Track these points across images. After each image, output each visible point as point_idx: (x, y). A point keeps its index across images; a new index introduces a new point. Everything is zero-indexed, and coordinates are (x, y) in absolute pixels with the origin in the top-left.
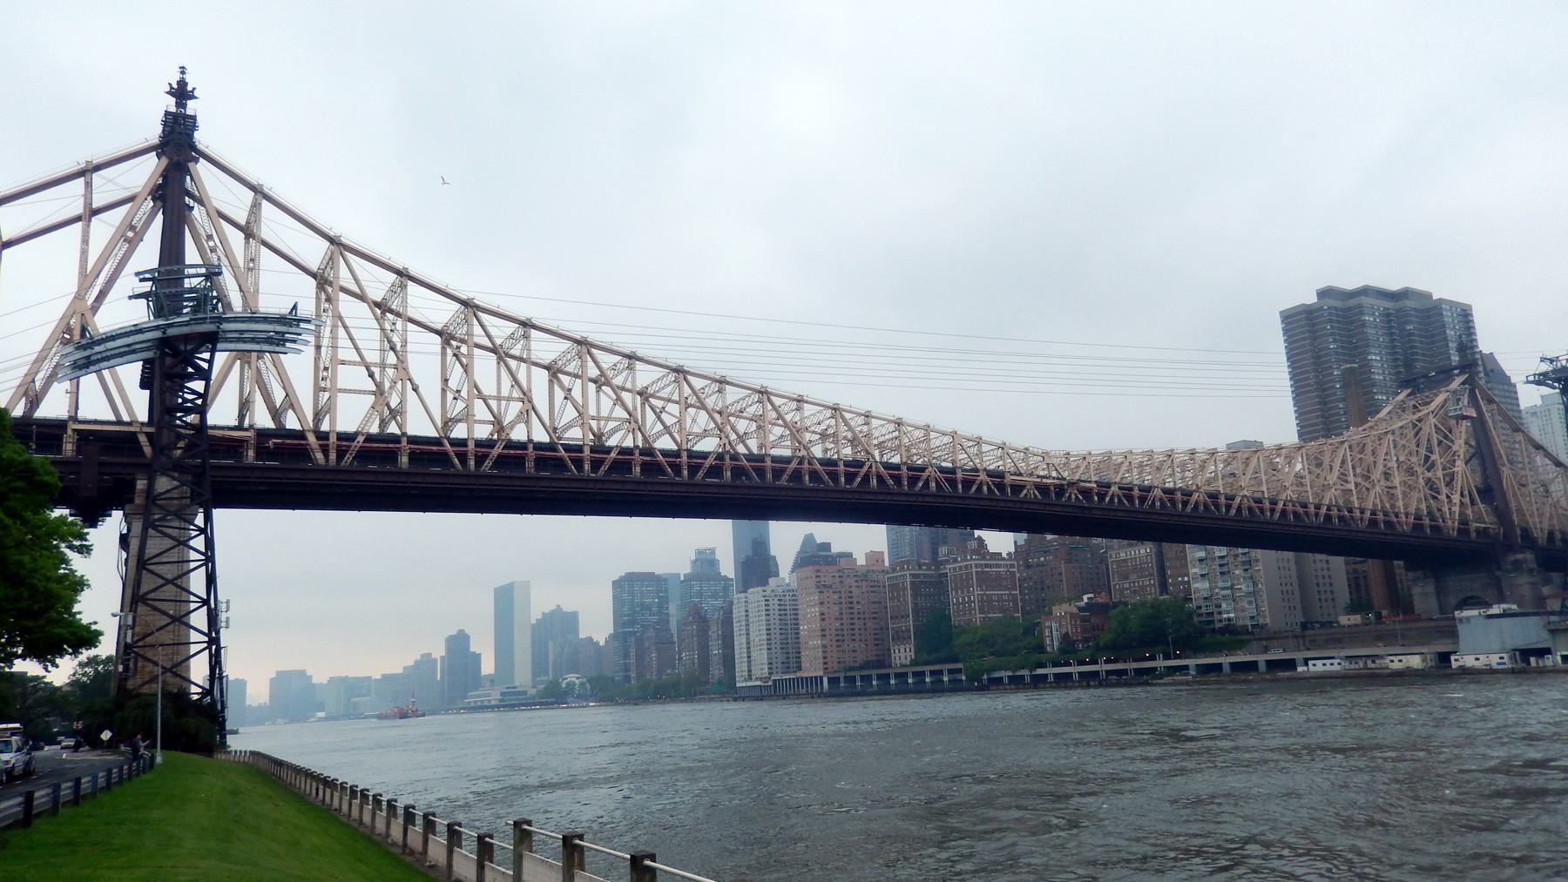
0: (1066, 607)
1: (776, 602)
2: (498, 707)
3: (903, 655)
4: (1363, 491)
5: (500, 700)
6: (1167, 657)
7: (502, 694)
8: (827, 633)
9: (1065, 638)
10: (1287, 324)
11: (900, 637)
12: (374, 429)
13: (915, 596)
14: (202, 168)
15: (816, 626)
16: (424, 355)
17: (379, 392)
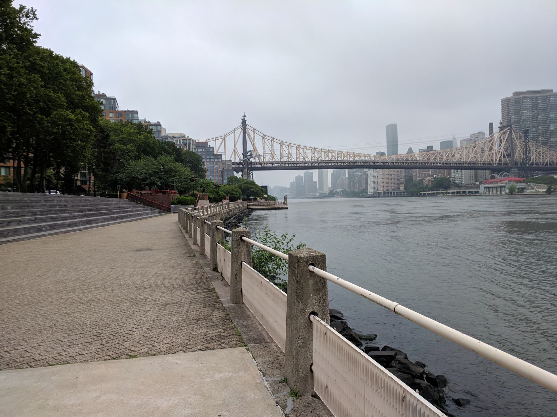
0: (429, 178)
1: (376, 173)
2: (317, 197)
3: (402, 188)
4: (481, 156)
5: (319, 195)
6: (441, 190)
7: (320, 194)
8: (384, 182)
9: (427, 185)
10: (503, 103)
11: (402, 183)
12: (271, 161)
13: (405, 173)
14: (248, 127)
15: (382, 180)
16: (277, 146)
17: (272, 154)
